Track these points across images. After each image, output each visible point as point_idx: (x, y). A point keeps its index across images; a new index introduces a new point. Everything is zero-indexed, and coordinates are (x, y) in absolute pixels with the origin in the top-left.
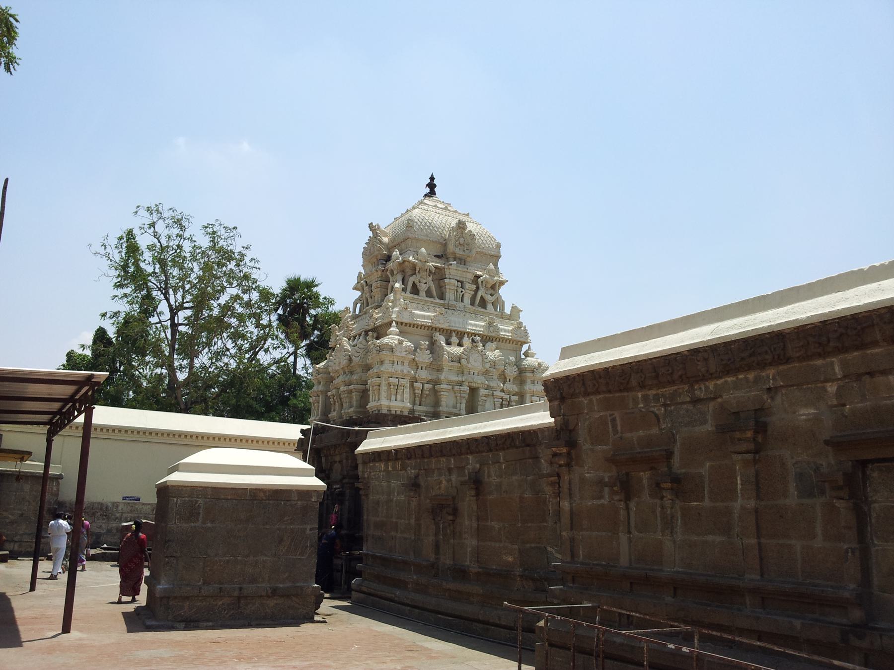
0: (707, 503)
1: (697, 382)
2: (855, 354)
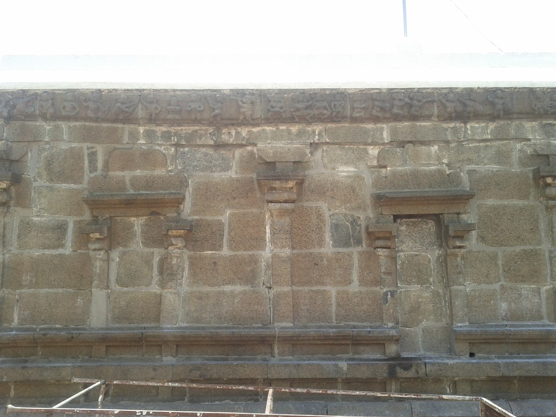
0: (225, 251)
1: (226, 126)
2: (406, 123)
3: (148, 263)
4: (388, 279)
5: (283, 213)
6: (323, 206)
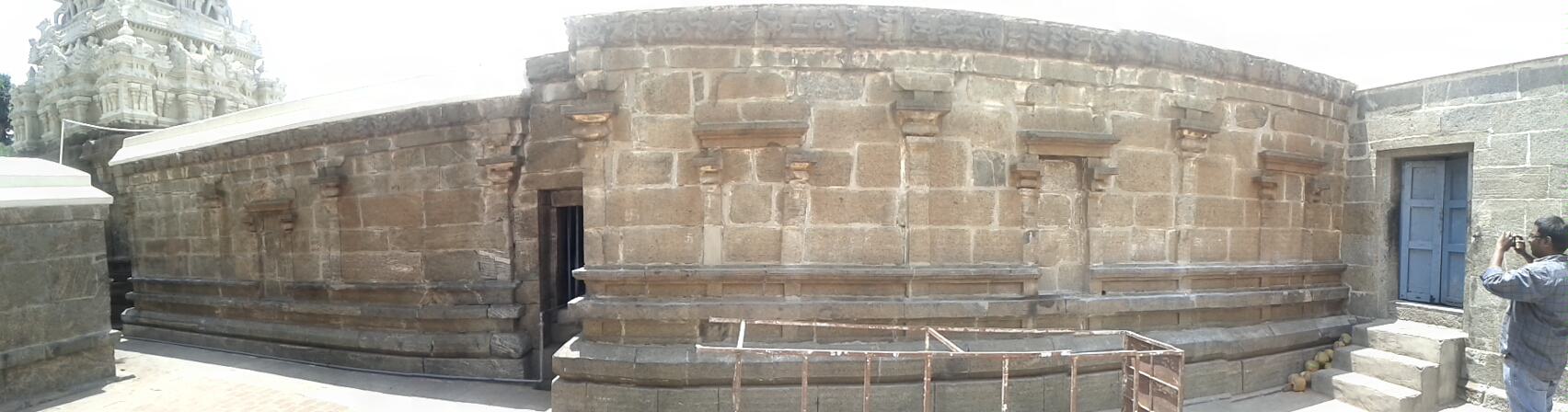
1: (858, 47)
3: (766, 198)
4: (1030, 218)
5: (920, 148)
6: (966, 142)
